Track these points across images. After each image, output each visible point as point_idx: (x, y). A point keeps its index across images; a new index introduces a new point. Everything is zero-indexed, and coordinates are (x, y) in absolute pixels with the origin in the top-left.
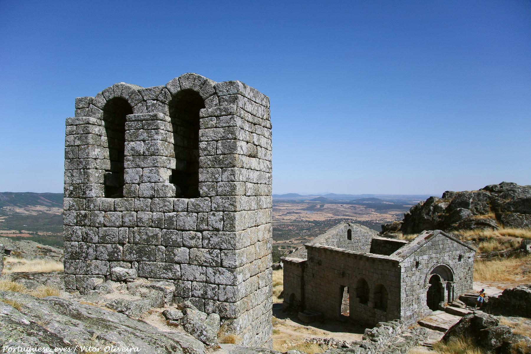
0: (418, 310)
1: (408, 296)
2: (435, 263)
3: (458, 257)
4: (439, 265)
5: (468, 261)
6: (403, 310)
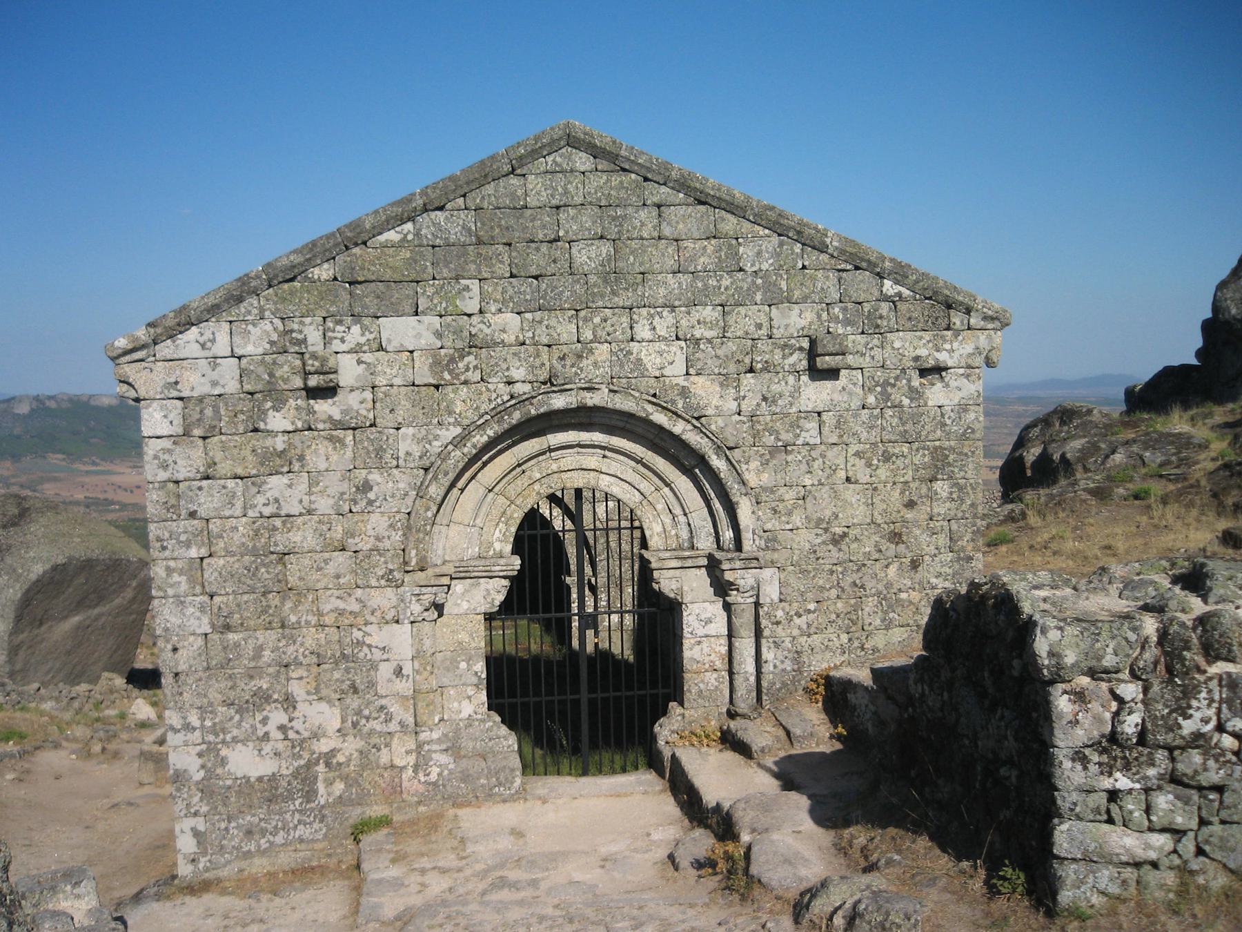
0: (351, 746)
1: (228, 628)
2: (520, 388)
5: (915, 394)
6: (188, 727)
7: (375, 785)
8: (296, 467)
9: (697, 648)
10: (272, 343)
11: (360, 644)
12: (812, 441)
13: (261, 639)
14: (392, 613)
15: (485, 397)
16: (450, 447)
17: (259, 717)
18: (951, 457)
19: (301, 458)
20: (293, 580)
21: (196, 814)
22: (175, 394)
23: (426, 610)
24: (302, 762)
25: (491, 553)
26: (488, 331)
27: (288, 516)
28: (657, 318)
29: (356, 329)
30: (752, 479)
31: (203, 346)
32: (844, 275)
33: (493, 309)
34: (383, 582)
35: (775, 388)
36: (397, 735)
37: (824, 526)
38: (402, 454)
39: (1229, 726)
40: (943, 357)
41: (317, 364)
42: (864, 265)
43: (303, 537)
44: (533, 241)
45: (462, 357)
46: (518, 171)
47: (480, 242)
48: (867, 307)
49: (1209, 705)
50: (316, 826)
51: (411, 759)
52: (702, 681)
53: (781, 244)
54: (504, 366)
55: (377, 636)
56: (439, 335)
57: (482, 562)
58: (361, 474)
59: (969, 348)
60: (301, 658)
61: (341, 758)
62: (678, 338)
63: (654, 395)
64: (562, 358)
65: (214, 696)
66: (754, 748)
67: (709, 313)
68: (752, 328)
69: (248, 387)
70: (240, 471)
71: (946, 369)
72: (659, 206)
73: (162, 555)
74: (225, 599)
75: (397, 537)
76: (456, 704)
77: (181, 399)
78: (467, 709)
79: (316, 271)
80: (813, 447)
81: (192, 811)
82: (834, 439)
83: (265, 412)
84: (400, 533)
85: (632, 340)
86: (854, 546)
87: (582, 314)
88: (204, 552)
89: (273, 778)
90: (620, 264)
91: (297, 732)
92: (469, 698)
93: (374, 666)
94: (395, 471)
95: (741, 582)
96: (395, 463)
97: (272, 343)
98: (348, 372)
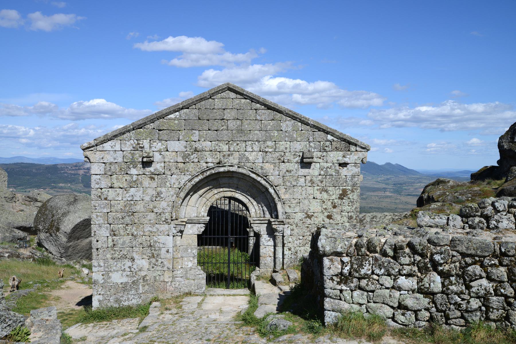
1: (115, 235)
3: (298, 159)
4: (222, 170)
5: (337, 172)
6: (100, 266)
7: (158, 287)
8: (139, 185)
9: (265, 249)
10: (134, 147)
11: (156, 242)
12: (302, 185)
13: (125, 239)
14: (167, 232)
15: (199, 167)
16: (187, 182)
17: (123, 263)
18: (349, 193)
19: (141, 183)
20: (136, 221)
21: (100, 294)
22: (102, 161)
23: (178, 232)
24: (135, 279)
25: (200, 215)
26: (201, 147)
27: (136, 201)
28: (254, 144)
29: (160, 144)
30: (283, 196)
31: (112, 147)
32: (315, 133)
33: (203, 140)
34: (164, 223)
35: (291, 168)
36: (166, 271)
37: (305, 212)
38: (172, 183)
39: (375, 272)
40: (346, 160)
41: (146, 154)
42: (321, 130)
43: (139, 207)
44: (216, 119)
45: (192, 154)
46: (212, 98)
47: (200, 119)
48: (322, 143)
49: (369, 265)
50: (138, 300)
51: (170, 279)
52: (266, 260)
53: (294, 123)
54: (205, 158)
55: (162, 239)
56: (186, 147)
57: (197, 218)
58: (159, 189)
59: (356, 157)
60: (137, 245)
61: (148, 278)
62: (260, 151)
63: (252, 169)
64: (224, 156)
65: (109, 256)
66: (277, 281)
67: (269, 143)
68: (284, 149)
69: (126, 161)
70: (122, 186)
71: (348, 164)
72: (256, 110)
73: (95, 211)
74: (114, 225)
75: (169, 209)
76: (187, 263)
77: (104, 163)
78: (190, 265)
79: (148, 126)
80: (302, 187)
81: (99, 293)
82: (310, 185)
83: (130, 168)
84: (170, 208)
85: (246, 151)
86: (316, 219)
87: (230, 142)
88: (109, 211)
89: (126, 283)
90: (243, 128)
91: (135, 269)
92: (191, 261)
93: (160, 249)
94: (170, 189)
95: (278, 229)
96: (170, 186)
97: (134, 147)
98: (157, 157)
